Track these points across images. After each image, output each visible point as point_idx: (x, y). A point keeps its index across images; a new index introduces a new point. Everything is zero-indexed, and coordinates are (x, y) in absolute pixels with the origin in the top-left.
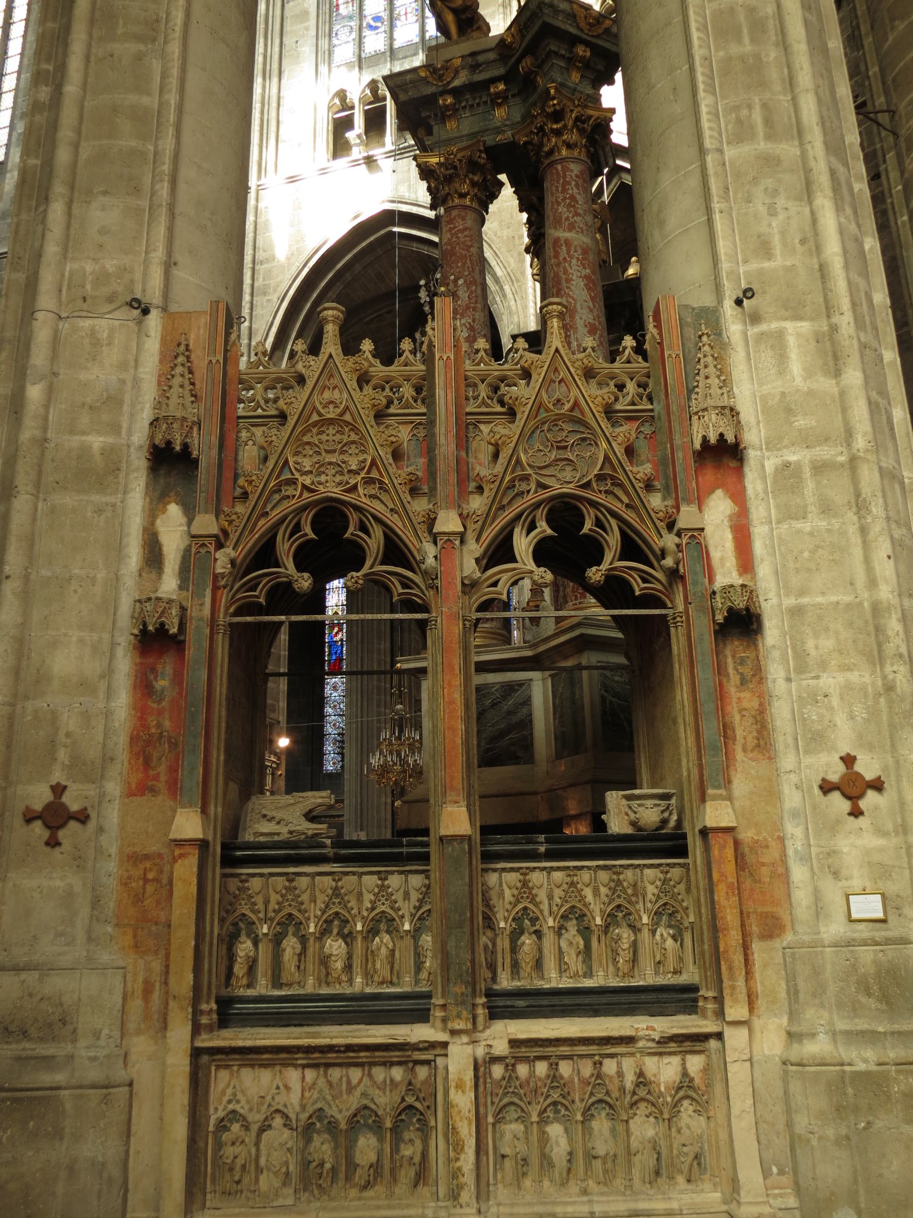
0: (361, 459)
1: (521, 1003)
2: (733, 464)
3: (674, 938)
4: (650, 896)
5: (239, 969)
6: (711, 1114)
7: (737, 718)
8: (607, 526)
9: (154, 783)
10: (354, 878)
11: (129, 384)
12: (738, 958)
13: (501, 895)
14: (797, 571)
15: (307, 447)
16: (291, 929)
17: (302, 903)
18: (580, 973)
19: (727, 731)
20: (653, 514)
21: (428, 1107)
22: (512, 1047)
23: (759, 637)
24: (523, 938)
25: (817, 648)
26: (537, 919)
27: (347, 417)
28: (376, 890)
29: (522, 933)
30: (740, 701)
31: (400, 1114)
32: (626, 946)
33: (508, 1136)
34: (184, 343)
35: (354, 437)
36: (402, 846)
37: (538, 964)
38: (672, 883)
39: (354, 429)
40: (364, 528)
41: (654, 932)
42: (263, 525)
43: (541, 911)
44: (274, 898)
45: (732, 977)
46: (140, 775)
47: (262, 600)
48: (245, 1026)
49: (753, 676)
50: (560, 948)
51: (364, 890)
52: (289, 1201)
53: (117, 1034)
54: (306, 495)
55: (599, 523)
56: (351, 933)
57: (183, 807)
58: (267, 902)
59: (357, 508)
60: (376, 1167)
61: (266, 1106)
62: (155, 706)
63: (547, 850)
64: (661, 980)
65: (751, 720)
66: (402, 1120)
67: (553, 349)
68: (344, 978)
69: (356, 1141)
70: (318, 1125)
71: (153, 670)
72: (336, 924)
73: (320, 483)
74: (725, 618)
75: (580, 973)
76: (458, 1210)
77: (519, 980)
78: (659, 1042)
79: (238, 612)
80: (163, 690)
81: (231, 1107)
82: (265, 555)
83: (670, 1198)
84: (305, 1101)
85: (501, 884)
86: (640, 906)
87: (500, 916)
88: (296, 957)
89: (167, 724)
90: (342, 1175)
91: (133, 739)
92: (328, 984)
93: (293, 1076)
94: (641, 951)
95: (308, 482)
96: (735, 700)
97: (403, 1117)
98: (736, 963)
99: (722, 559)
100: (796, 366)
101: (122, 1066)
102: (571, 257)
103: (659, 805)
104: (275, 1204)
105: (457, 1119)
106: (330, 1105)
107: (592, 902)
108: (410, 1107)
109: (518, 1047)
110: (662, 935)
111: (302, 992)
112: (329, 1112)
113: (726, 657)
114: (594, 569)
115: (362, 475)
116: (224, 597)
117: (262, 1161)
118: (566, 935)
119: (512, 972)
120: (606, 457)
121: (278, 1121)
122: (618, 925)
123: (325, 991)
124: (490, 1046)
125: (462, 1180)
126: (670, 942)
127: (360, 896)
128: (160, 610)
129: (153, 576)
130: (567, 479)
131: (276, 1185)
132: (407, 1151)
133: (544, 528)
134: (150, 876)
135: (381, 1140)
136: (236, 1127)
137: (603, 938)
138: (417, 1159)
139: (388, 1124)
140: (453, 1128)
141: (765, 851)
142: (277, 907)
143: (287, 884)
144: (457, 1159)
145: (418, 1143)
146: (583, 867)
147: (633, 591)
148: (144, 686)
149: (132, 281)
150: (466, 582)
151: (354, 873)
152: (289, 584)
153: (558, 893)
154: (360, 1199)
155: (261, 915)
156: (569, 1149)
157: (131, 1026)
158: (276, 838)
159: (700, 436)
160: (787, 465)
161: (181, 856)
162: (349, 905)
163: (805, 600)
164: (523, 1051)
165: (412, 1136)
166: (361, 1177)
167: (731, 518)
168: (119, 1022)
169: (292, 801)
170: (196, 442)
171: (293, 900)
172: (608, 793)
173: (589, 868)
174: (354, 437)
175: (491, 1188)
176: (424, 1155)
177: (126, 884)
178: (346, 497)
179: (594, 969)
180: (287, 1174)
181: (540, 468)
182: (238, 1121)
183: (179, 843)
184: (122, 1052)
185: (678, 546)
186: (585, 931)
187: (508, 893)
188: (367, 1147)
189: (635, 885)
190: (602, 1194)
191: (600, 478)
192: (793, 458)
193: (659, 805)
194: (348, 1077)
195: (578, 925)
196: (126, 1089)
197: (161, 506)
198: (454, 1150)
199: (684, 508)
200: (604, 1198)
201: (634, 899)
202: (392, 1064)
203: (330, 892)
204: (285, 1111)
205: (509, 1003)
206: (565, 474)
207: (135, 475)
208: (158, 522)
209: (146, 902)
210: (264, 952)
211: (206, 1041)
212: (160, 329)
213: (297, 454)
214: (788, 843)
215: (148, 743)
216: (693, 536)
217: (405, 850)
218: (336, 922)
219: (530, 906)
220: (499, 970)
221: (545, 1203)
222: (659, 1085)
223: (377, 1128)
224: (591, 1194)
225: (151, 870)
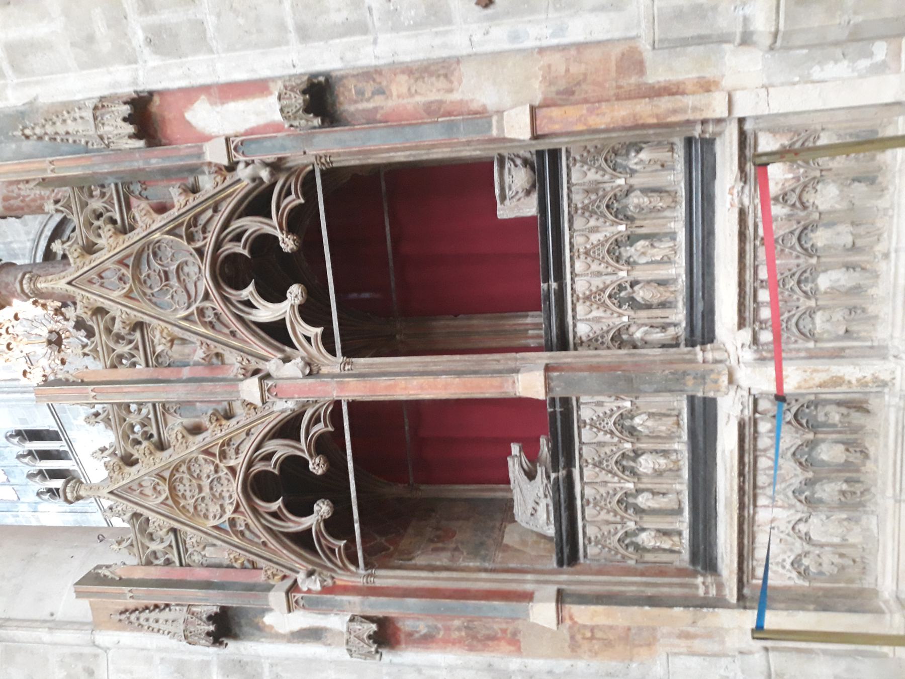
0: (203, 462)
1: (699, 307)
2: (157, 99)
3: (639, 151)
4: (598, 177)
5: (666, 544)
6: (819, 127)
7: (419, 99)
8: (238, 231)
9: (509, 632)
10: (584, 448)
11: (164, 655)
12: (665, 103)
13: (598, 320)
14: (260, 31)
15: (199, 508)
16: (631, 500)
17: (608, 493)
18: (671, 244)
19: (433, 110)
20: (219, 188)
21: (797, 400)
22: (745, 326)
23: (334, 74)
24: (638, 299)
25: (339, 10)
26: (620, 285)
27: (167, 474)
28: (595, 430)
29: (633, 299)
30: (402, 97)
31: (801, 425)
32: (646, 199)
33: (828, 326)
34: (119, 617)
35: (184, 468)
36: (554, 413)
38: (585, 154)
39: (177, 469)
40: (268, 457)
41: (633, 172)
42: (273, 543)
43: (612, 283)
44: (604, 516)
45: (684, 110)
46: (503, 643)
47: (342, 543)
48: (716, 544)
49: (374, 80)
50: (647, 263)
51: (595, 441)
52: (874, 520)
53: (724, 661)
54: (242, 509)
55: (237, 238)
56: (634, 451)
57: (528, 615)
58: (608, 523)
59: (250, 464)
60: (849, 445)
61: (788, 538)
62: (442, 633)
63: (555, 281)
64: (680, 166)
65: (420, 83)
66: (807, 422)
67: (69, 287)
68: (674, 457)
69: (823, 461)
70: (807, 493)
71: (410, 634)
72: (626, 465)
73: (231, 497)
74: (316, 115)
75: (671, 244)
76: (898, 382)
77: (677, 301)
78: (745, 182)
79: (354, 561)
80: (428, 626)
81: (788, 566)
82: (303, 540)
84: (786, 505)
85: (588, 320)
86: (608, 187)
87: (617, 321)
88: (655, 497)
89: (457, 623)
90: (854, 475)
91: (471, 649)
92: (679, 470)
93: (763, 516)
95: (232, 508)
96: (400, 100)
97: (804, 422)
98: (670, 106)
99: (257, 114)
100: (41, 30)
101: (750, 656)
102: (19, 195)
103: (509, 170)
104: (875, 531)
105: (811, 383)
106: (791, 485)
107: (603, 234)
108: (795, 416)
109: (745, 319)
110: (636, 164)
111: (686, 493)
112: (796, 485)
113: (357, 110)
114: (282, 245)
115: (217, 461)
116: (343, 579)
117: (837, 540)
118: (635, 258)
119: (669, 308)
120: (169, 233)
121: (802, 527)
122: (627, 206)
123: (685, 473)
124: (743, 345)
125: (869, 378)
126: (643, 155)
127: (601, 444)
128: (357, 641)
129: (328, 635)
130: (197, 270)
131: (859, 530)
132: (835, 417)
133: (249, 292)
134: (589, 634)
135: (823, 441)
136: (806, 562)
138: (844, 410)
139: (810, 436)
140: (820, 386)
141: (553, 69)
142: (612, 514)
143: (591, 505)
144: (849, 382)
145: (828, 408)
146: (570, 243)
147: (300, 205)
148: (426, 640)
149: (72, 655)
150: (307, 371)
151: (580, 449)
152: (326, 522)
153: (595, 267)
154: (876, 461)
155: (619, 526)
156: (844, 269)
157: (716, 648)
158: (551, 508)
159: (130, 141)
160: (149, 41)
161: (571, 618)
162: (609, 453)
163: (290, 23)
164: (749, 315)
165: (823, 414)
166: (856, 458)
167: (213, 104)
168: (714, 659)
169: (518, 489)
170: (206, 608)
171: (605, 500)
172: (499, 217)
173: (571, 237)
174: (184, 468)
175: (876, 344)
176: (839, 403)
177: (596, 654)
178: (241, 476)
179: (668, 230)
180: (849, 519)
181: (189, 296)
182: (801, 560)
183: (560, 620)
184: (739, 656)
185: (247, 164)
186: (631, 239)
187: (596, 313)
188: (830, 452)
189: (587, 192)
190: (890, 237)
191: (190, 238)
192: (140, 36)
193: (509, 170)
194: (766, 469)
195: (626, 246)
196: (771, 654)
197: (267, 629)
198: (840, 385)
199: (208, 158)
202: (756, 431)
203: (597, 469)
204: (793, 522)
205: (700, 316)
206: (192, 273)
207: (242, 650)
208: (282, 631)
209: (612, 637)
210: (651, 522)
211: (732, 595)
212: (110, 632)
213: (206, 517)
214: (545, 43)
215: (474, 637)
216: (236, 149)
217: (558, 409)
218: (624, 463)
219: (608, 292)
220: (667, 321)
221: (895, 295)
222: (786, 180)
223: (812, 445)
224: (889, 250)
225: (584, 634)
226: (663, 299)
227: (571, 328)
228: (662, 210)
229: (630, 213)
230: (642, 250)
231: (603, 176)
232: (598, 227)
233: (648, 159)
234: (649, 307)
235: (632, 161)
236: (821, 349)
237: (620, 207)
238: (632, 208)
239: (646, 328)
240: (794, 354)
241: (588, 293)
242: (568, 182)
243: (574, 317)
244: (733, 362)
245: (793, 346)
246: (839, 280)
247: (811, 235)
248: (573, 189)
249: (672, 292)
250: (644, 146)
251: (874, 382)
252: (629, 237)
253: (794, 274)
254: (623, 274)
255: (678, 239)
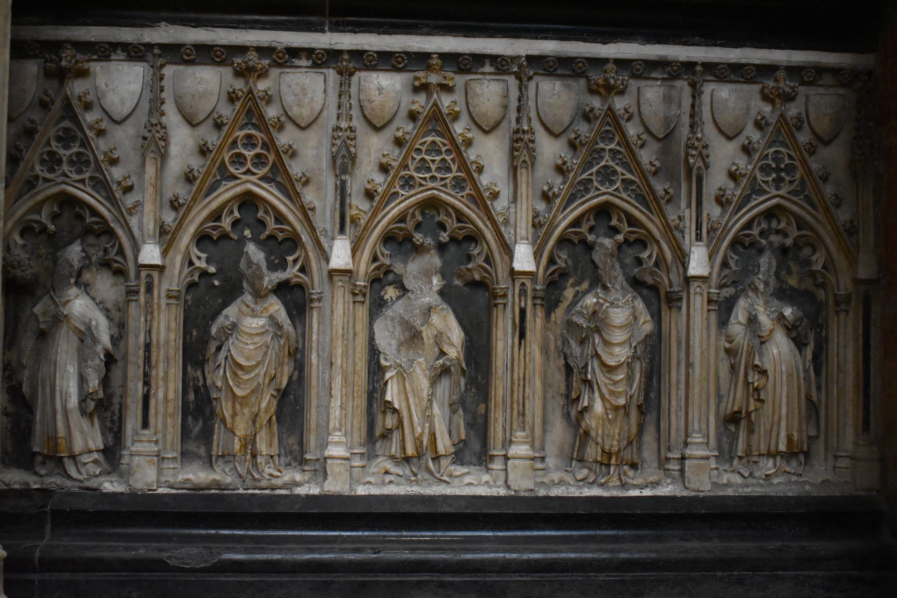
13: (155, 143)
18: (444, 444)
24: (231, 312)
26: (294, 242)
29: (231, 291)
32: (621, 354)
37: (291, 407)
38: (803, 138)
41: (723, 309)
43: (306, 212)
50: (374, 352)
75: (444, 444)
77: (209, 462)
85: (156, 105)
86: (682, 212)
87: (145, 222)
94: (675, 375)
110: (752, 321)
119: (185, 433)
122: (597, 281)
126: (780, 349)
137: (536, 322)
146: (479, 59)
153: (374, 148)
173: (501, 64)
179: (497, 431)
187: (182, 141)
189: (667, 139)
201: (659, 187)
205: (142, 551)
219: (270, 194)
220: (132, 422)
226: (226, 408)
227: (127, 35)
228: (575, 418)
229: (569, 293)
230: (427, 334)
231: (721, 201)
232: (532, 163)
233: (768, 366)
234: (197, 350)
235: (759, 308)
237: (597, 257)
238: (590, 300)
239: (105, 339)
241: (272, 112)
242: (710, 68)
243: (174, 53)
248: (683, 86)
249: (250, 443)
250: (809, 352)
252: (480, 285)
254: (340, 254)
255: (459, 470)
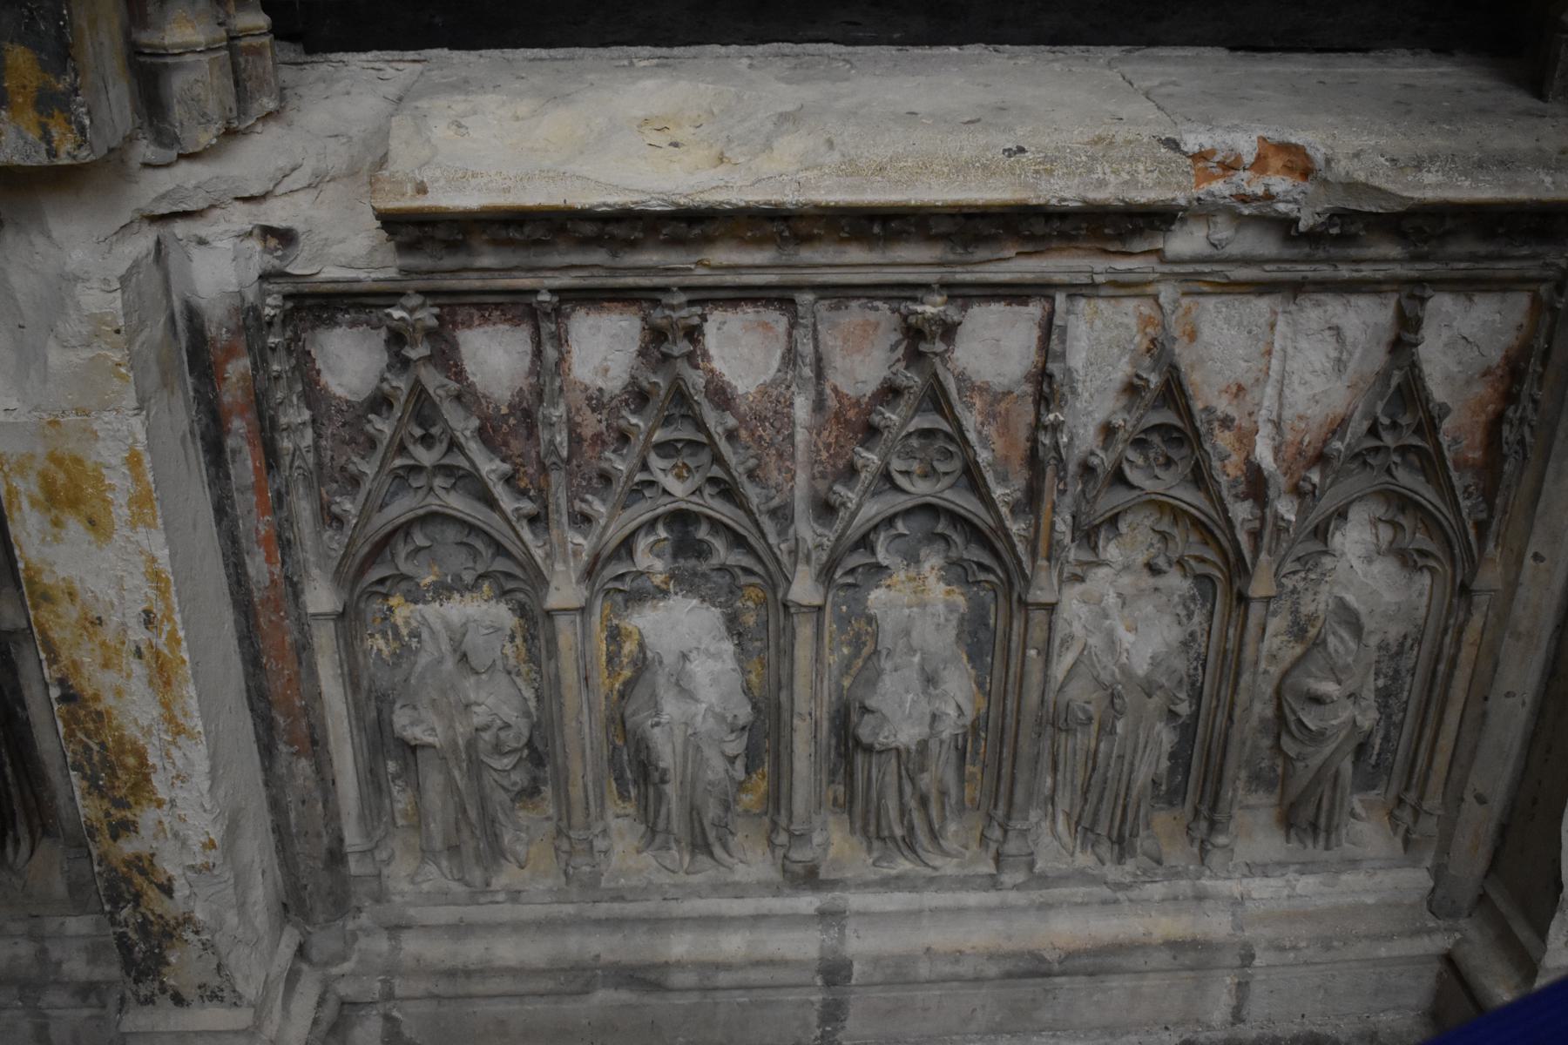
22: (405, 248)
78: (1314, 237)
83: (1200, 897)
105: (88, 658)
124: (285, 237)
164: (488, 266)
190: (887, 884)
200: (897, 900)
221: (616, 923)
222: (1246, 439)
224: (832, 884)
236: (304, 648)
240: (254, 522)
244: (154, 189)
245: (303, 507)
246: (685, 692)
247: (932, 562)
251: (144, 927)
253: (728, 491)
